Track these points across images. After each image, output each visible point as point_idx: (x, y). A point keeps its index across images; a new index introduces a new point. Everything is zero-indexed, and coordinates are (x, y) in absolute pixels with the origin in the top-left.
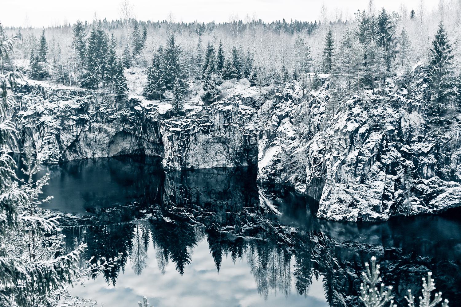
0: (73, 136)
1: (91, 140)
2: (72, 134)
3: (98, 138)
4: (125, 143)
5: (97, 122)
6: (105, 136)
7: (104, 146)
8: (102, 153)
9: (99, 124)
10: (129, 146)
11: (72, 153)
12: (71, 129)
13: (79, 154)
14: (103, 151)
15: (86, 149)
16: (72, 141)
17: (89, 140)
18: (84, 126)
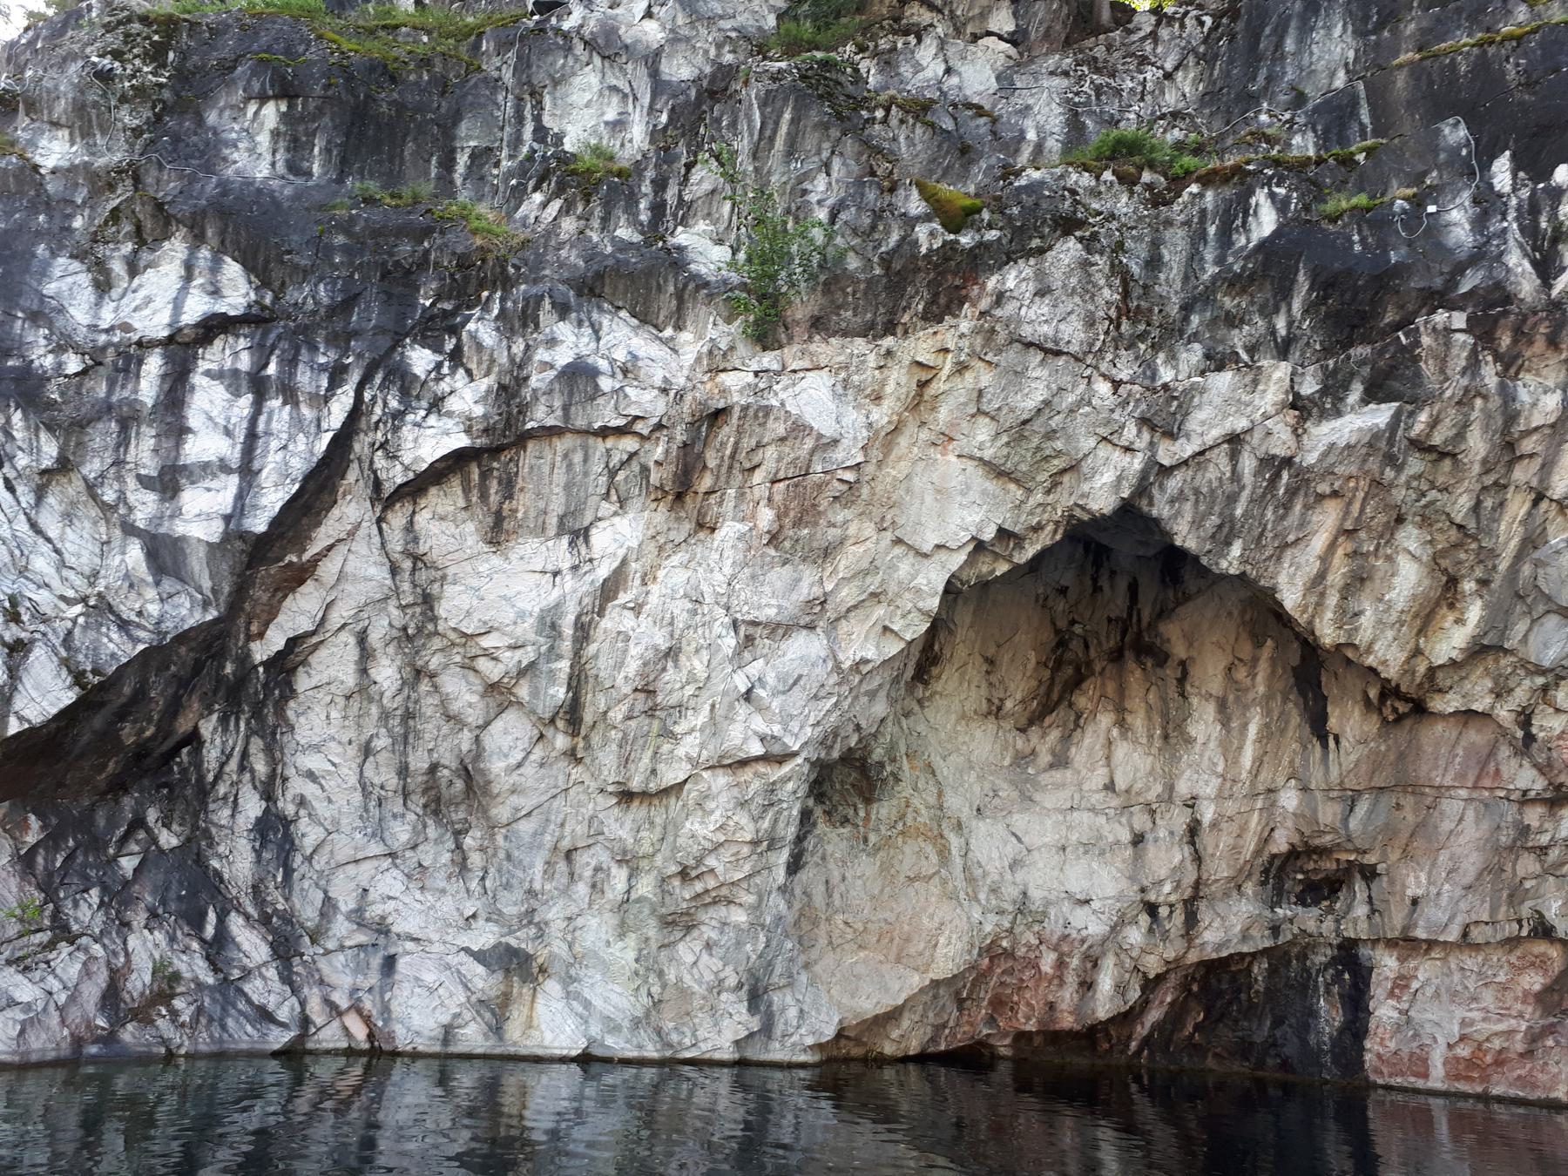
0: (165, 555)
1: (498, 694)
2: (145, 505)
3: (629, 640)
4: (1040, 829)
5: (646, 284)
6: (771, 597)
7: (716, 819)
8: (648, 966)
9: (709, 330)
10: (1107, 883)
11: (86, 911)
12: (128, 420)
13: (251, 944)
14: (679, 923)
15: (390, 882)
16: (116, 648)
17: (463, 694)
18: (402, 378)
